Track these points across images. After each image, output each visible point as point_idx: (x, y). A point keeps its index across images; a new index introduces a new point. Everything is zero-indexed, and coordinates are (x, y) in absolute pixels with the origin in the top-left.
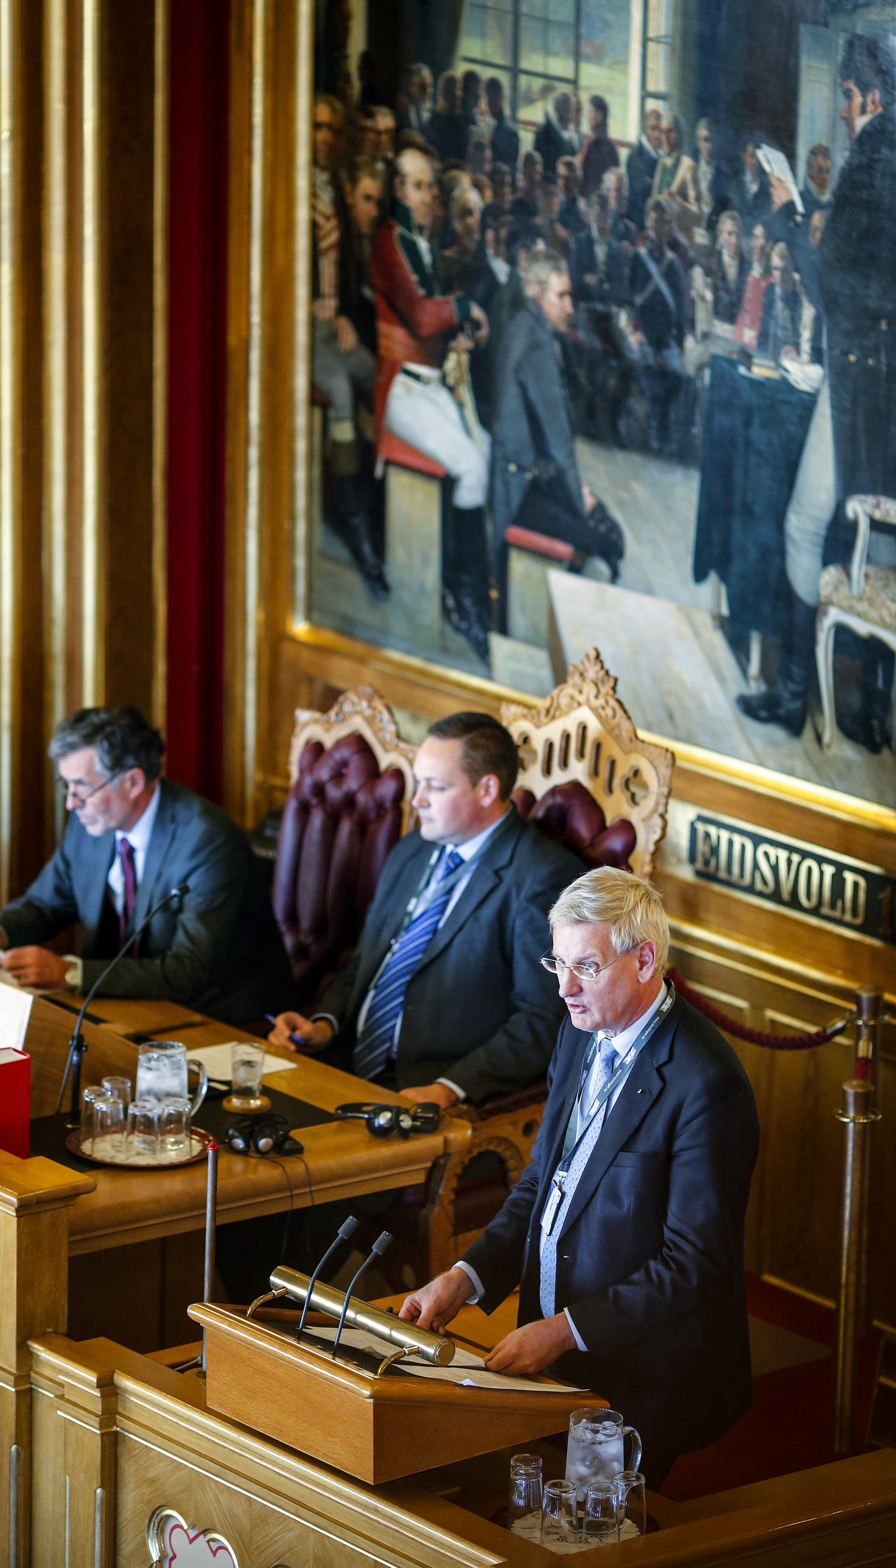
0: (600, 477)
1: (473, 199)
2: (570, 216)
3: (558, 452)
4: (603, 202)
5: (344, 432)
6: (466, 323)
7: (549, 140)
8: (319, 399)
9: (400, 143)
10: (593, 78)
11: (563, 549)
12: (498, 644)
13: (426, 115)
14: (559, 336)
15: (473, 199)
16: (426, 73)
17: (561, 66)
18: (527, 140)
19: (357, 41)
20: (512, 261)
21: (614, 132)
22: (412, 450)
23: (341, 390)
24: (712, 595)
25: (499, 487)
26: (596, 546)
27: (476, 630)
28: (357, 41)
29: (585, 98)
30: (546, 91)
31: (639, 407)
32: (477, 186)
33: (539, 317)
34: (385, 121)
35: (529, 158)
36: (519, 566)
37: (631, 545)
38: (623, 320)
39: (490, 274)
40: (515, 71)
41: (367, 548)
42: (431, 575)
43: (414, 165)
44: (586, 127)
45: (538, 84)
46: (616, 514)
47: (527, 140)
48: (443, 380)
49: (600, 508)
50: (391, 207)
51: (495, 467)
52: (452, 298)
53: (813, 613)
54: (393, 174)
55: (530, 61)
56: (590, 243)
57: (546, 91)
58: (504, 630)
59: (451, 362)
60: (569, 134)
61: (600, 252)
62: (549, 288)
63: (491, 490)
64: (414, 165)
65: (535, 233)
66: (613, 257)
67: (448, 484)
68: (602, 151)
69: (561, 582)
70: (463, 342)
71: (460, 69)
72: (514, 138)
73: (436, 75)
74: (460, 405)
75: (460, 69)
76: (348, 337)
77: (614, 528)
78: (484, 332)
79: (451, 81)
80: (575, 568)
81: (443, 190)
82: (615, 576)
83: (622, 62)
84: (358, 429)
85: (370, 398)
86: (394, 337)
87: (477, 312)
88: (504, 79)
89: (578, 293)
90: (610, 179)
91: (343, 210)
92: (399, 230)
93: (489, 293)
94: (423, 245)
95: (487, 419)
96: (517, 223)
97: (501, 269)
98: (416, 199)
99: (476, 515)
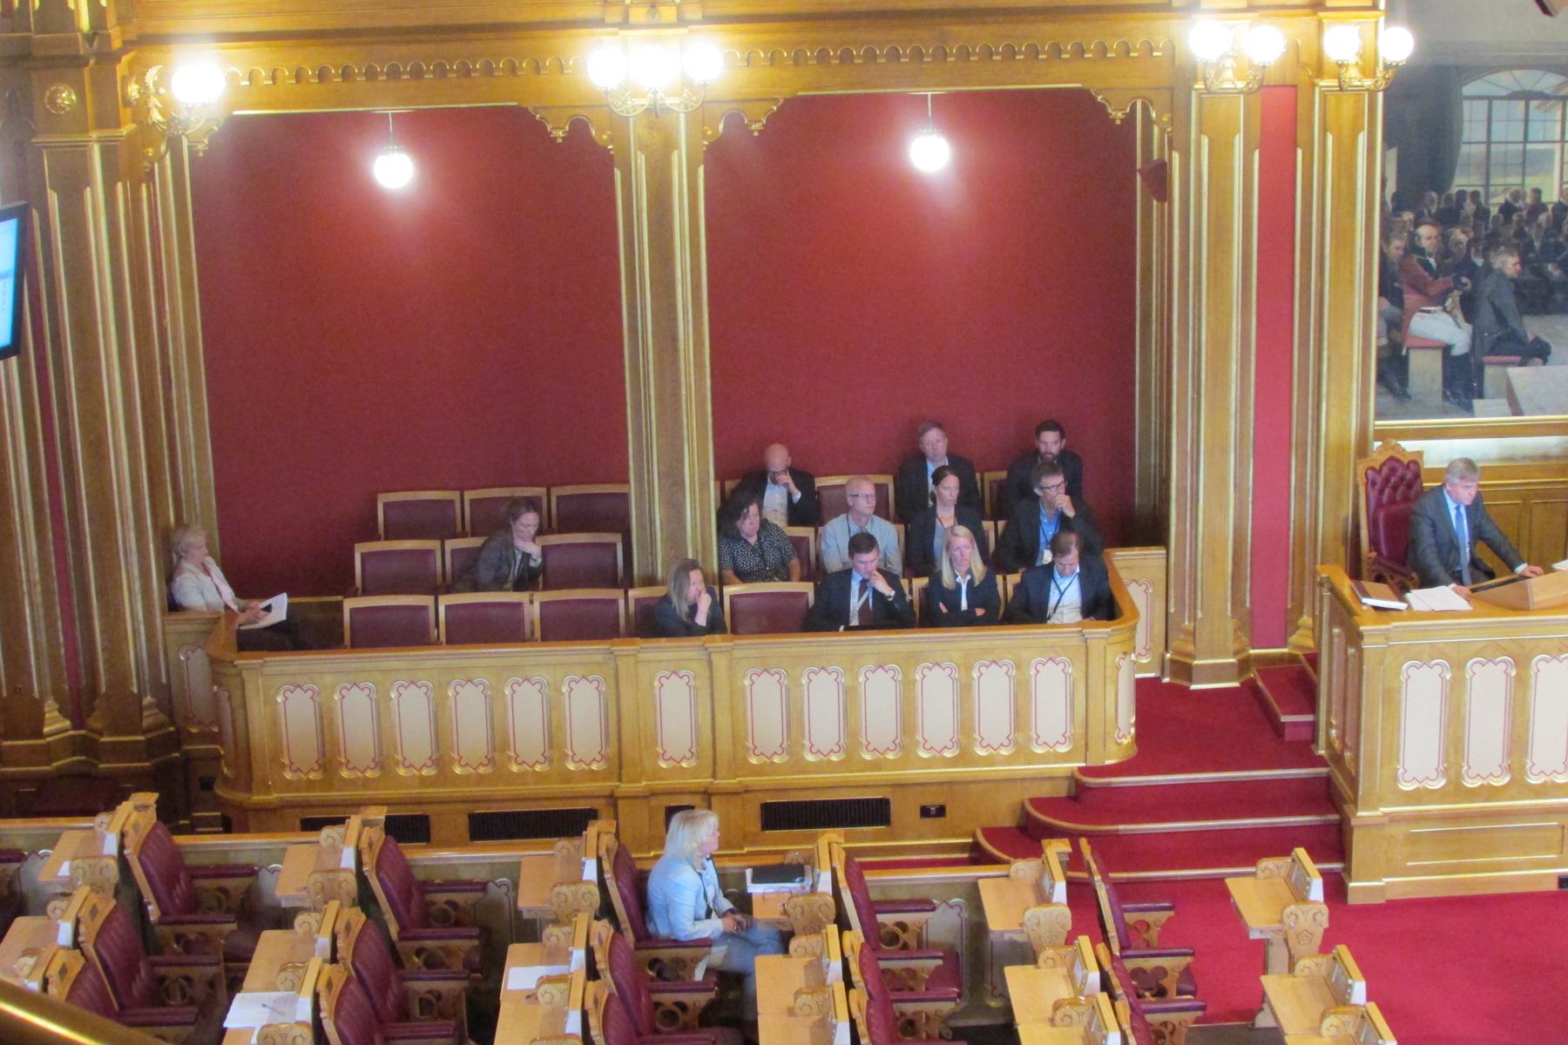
0: (1534, 327)
1: (1462, 238)
2: (1520, 234)
3: (1514, 324)
4: (1539, 226)
6: (1458, 284)
7: (1507, 209)
9: (1417, 223)
10: (1532, 182)
11: (1517, 359)
12: (1477, 403)
13: (1434, 211)
14: (1512, 280)
15: (1462, 238)
16: (1434, 195)
17: (1514, 180)
18: (1494, 211)
20: (1486, 257)
21: (1544, 199)
22: (1424, 339)
25: (1478, 343)
26: (1539, 352)
27: (1464, 400)
29: (1528, 190)
30: (1504, 191)
31: (1559, 297)
32: (1464, 232)
33: (1502, 275)
34: (1408, 216)
35: (1496, 217)
36: (1489, 372)
37: (1554, 348)
38: (1550, 267)
39: (1474, 265)
40: (1487, 186)
41: (1396, 385)
42: (1438, 385)
43: (1426, 232)
44: (1529, 200)
45: (1500, 189)
46: (1546, 339)
47: (1494, 211)
48: (1445, 310)
49: (1537, 340)
50: (1413, 247)
51: (1474, 337)
52: (1450, 278)
54: (1413, 236)
55: (1496, 180)
56: (1532, 242)
57: (1504, 191)
58: (1481, 396)
59: (1449, 303)
60: (1519, 204)
61: (1537, 244)
62: (1508, 263)
63: (1473, 346)
65: (1498, 245)
66: (1544, 245)
67: (1446, 349)
68: (1538, 207)
69: (1514, 372)
70: (1457, 293)
71: (1454, 190)
72: (1487, 212)
73: (1440, 195)
74: (1454, 317)
75: (1454, 190)
77: (1547, 345)
78: (1469, 286)
79: (1449, 198)
80: (1522, 364)
81: (1444, 238)
82: (1545, 362)
83: (1549, 172)
84: (1390, 339)
86: (1410, 298)
87: (1464, 280)
88: (1481, 190)
89: (1524, 262)
90: (1542, 218)
92: (1416, 257)
93: (1472, 271)
94: (1432, 261)
95: (1468, 319)
96: (1491, 242)
97: (1479, 262)
98: (1425, 243)
99: (1465, 356)
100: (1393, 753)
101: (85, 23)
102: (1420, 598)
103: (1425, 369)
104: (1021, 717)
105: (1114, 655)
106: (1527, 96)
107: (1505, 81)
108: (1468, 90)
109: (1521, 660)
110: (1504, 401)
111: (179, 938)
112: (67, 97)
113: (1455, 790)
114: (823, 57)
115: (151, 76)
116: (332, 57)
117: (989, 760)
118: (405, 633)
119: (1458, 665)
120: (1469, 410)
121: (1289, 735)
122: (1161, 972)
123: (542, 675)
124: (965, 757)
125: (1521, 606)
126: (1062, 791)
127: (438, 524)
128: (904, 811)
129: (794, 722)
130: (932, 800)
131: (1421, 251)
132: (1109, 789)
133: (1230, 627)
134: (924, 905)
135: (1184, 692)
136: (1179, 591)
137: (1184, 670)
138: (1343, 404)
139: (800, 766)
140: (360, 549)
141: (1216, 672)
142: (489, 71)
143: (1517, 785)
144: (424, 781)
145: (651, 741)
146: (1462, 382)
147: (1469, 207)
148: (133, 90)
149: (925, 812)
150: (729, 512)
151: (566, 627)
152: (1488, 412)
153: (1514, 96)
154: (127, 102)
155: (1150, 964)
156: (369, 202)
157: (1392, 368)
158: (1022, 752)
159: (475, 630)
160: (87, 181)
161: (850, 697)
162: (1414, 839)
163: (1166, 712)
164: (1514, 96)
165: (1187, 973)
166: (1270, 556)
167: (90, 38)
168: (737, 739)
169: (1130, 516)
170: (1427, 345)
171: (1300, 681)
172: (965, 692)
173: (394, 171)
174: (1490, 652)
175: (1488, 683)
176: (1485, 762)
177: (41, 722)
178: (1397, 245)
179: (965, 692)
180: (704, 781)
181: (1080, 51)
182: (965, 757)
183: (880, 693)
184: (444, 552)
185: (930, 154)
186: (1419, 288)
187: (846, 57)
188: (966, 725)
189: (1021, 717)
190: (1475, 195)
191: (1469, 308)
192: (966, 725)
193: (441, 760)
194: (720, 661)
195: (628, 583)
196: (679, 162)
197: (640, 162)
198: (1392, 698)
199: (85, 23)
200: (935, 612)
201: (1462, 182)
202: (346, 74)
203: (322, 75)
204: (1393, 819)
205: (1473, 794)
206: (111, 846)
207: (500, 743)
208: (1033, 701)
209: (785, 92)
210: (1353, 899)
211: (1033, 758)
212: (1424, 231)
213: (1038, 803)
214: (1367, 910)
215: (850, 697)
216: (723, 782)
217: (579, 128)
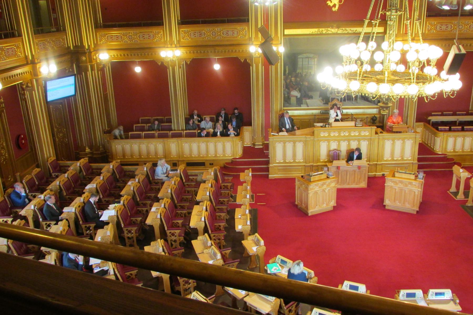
5: (286, 96)
8: (284, 94)
9: (292, 77)
19: (287, 72)
23: (286, 93)
24: (321, 98)
28: (287, 72)
34: (290, 76)
36: (303, 100)
50: (291, 81)
53: (329, 98)
55: (304, 71)
64: (293, 79)
67: (297, 97)
76: (287, 90)
85: (289, 93)
86: (291, 89)
91: (286, 82)
100: (275, 156)
101: (87, 47)
102: (281, 134)
103: (293, 100)
104: (224, 150)
105: (238, 142)
106: (308, 58)
107: (305, 55)
108: (299, 57)
109: (294, 143)
110: (306, 105)
111: (88, 178)
112: (84, 58)
113: (285, 162)
114: (197, 52)
115: (97, 55)
116: (126, 53)
117: (219, 157)
118: (139, 137)
119: (285, 143)
120: (300, 106)
121: (266, 154)
122: (227, 186)
123: (154, 143)
124: (216, 156)
125: (295, 135)
126: (230, 161)
127: (148, 122)
128: (207, 164)
129: (191, 150)
130: (211, 162)
131: (292, 82)
132: (236, 161)
133: (261, 138)
134: (196, 175)
135: (253, 148)
136: (253, 132)
137: (254, 144)
138: (277, 104)
139: (192, 157)
140: (134, 126)
141: (259, 145)
142: (148, 54)
143: (294, 162)
144: (138, 158)
145: (170, 153)
146: (299, 102)
147: (300, 75)
148: (95, 57)
149: (210, 164)
150: (187, 121)
151: (161, 136)
152: (303, 107)
153: (306, 58)
154: (94, 59)
155: (226, 184)
156: (135, 74)
157: (287, 100)
158: (224, 156)
159: (147, 137)
160: (88, 70)
161: (199, 147)
162: (279, 169)
163: (248, 151)
164: (306, 58)
165: (231, 186)
166: (267, 127)
167: (87, 50)
168: (183, 153)
169: (244, 120)
170: (294, 96)
171: (266, 147)
172: (215, 146)
173: (138, 70)
174: (289, 141)
175: (289, 146)
176: (289, 158)
177: (85, 150)
178: (288, 81)
179: (215, 146)
180: (178, 159)
181: (236, 51)
182: (216, 156)
183: (203, 146)
184: (147, 126)
185: (217, 67)
186: (292, 87)
187: (201, 52)
188: (216, 151)
189: (224, 150)
190: (300, 73)
191: (300, 91)
192: (216, 151)
193: (140, 155)
194: (179, 142)
195: (171, 130)
196: (177, 68)
197: (171, 68)
198: (274, 148)
199: (87, 47)
200: (215, 135)
201: (298, 71)
202: (128, 55)
203: (124, 55)
204: (275, 166)
205: (288, 163)
206: (78, 165)
207: (148, 153)
208: (227, 148)
209: (192, 58)
210: (270, 178)
211: (226, 157)
212: (293, 79)
213: (226, 163)
214: (271, 180)
215: (199, 147)
216: (180, 159)
217: (162, 63)
